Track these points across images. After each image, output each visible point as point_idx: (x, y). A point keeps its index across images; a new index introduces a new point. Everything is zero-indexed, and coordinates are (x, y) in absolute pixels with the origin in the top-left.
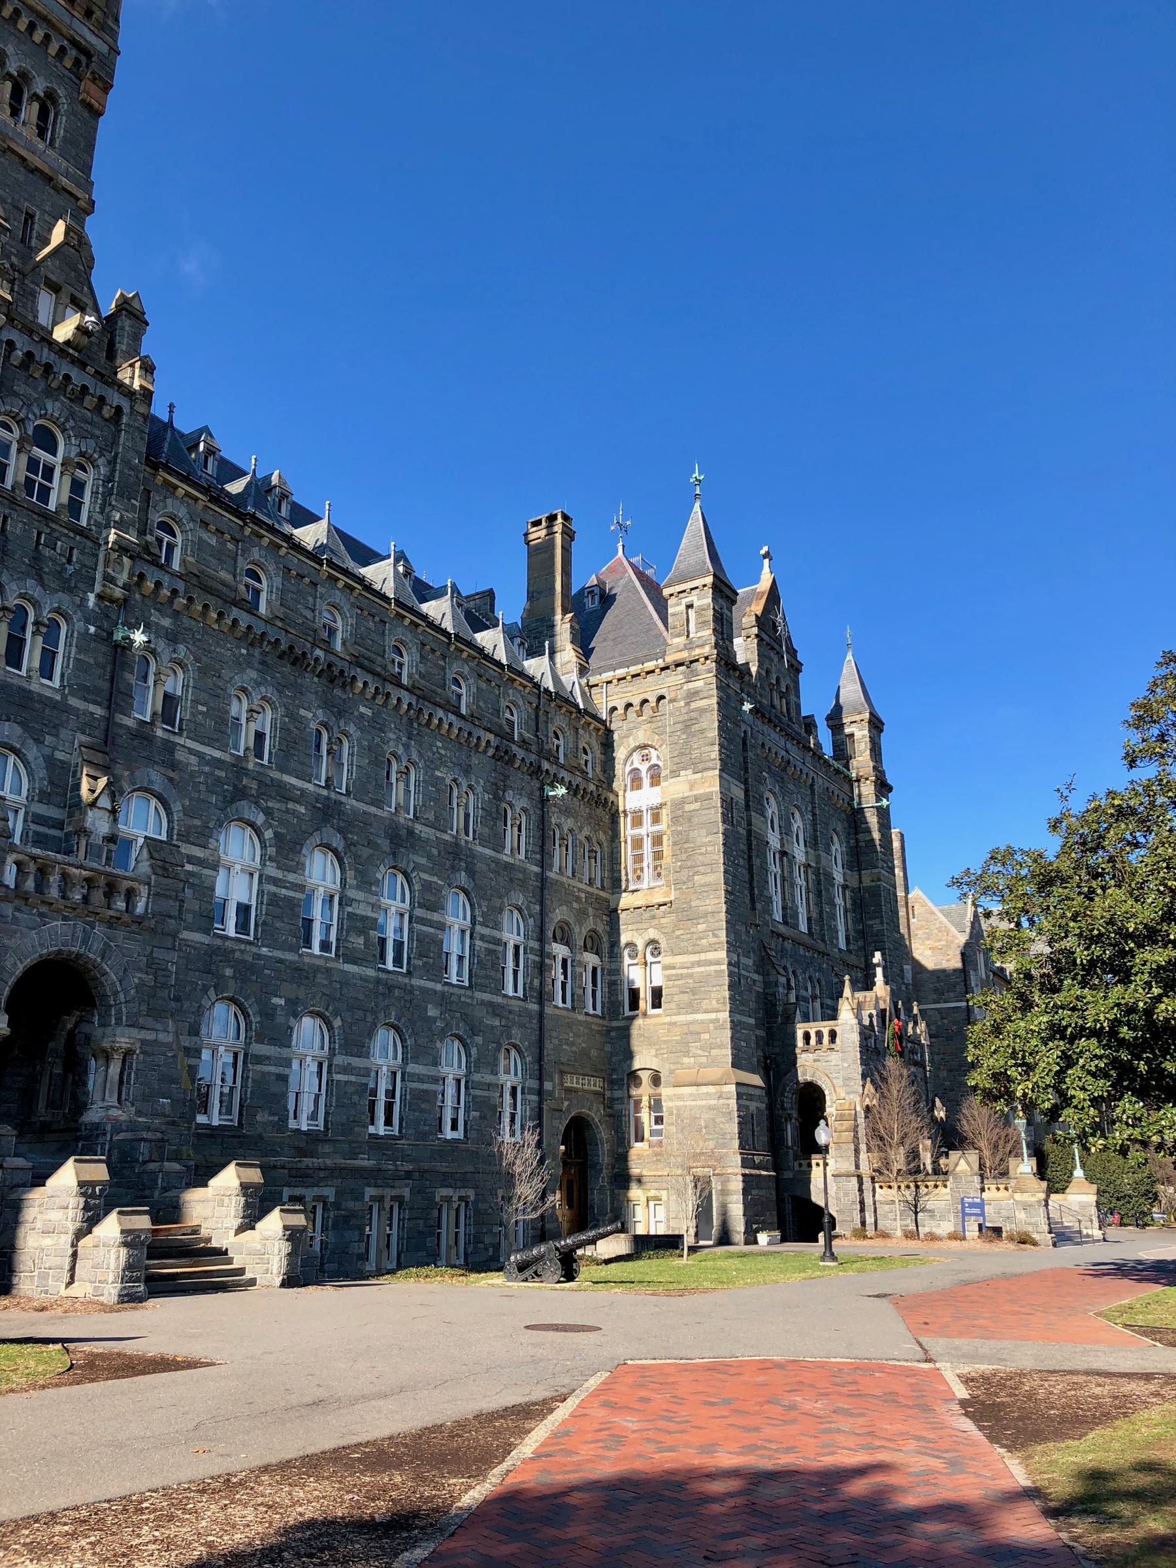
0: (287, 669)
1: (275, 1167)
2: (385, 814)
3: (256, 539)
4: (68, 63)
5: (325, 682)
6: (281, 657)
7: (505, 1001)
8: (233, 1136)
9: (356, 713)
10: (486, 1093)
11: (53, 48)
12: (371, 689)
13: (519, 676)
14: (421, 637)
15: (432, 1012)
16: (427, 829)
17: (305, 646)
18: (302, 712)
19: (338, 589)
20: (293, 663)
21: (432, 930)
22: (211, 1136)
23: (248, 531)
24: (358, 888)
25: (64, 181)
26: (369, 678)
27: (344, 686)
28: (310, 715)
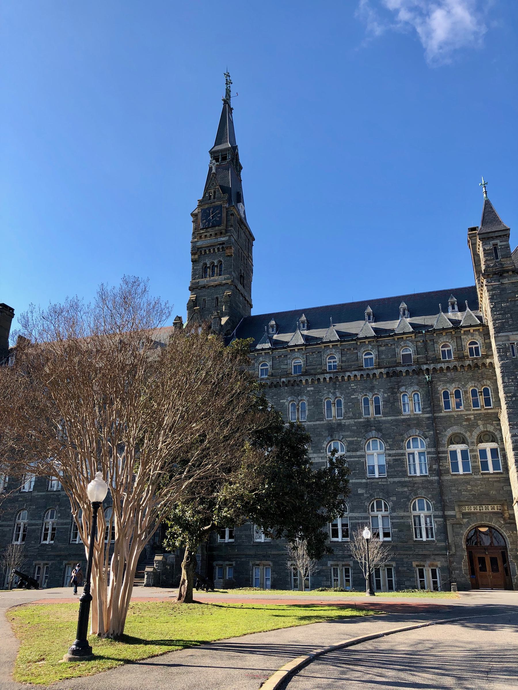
0: (274, 390)
1: (282, 555)
2: (325, 422)
3: (261, 355)
4: (221, 250)
5: (291, 387)
6: (270, 387)
7: (411, 479)
8: (266, 545)
9: (306, 392)
10: (402, 521)
11: (216, 251)
12: (310, 381)
13: (403, 335)
14: (340, 348)
15: (360, 491)
16: (350, 420)
17: (276, 380)
18: (281, 401)
19: (296, 352)
20: (275, 387)
21: (357, 459)
22: (257, 546)
23: (256, 355)
24: (314, 453)
25: (224, 282)
26: (307, 378)
27: (298, 385)
28: (285, 401)
